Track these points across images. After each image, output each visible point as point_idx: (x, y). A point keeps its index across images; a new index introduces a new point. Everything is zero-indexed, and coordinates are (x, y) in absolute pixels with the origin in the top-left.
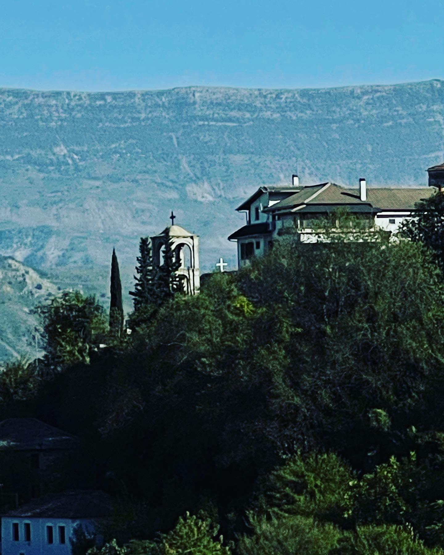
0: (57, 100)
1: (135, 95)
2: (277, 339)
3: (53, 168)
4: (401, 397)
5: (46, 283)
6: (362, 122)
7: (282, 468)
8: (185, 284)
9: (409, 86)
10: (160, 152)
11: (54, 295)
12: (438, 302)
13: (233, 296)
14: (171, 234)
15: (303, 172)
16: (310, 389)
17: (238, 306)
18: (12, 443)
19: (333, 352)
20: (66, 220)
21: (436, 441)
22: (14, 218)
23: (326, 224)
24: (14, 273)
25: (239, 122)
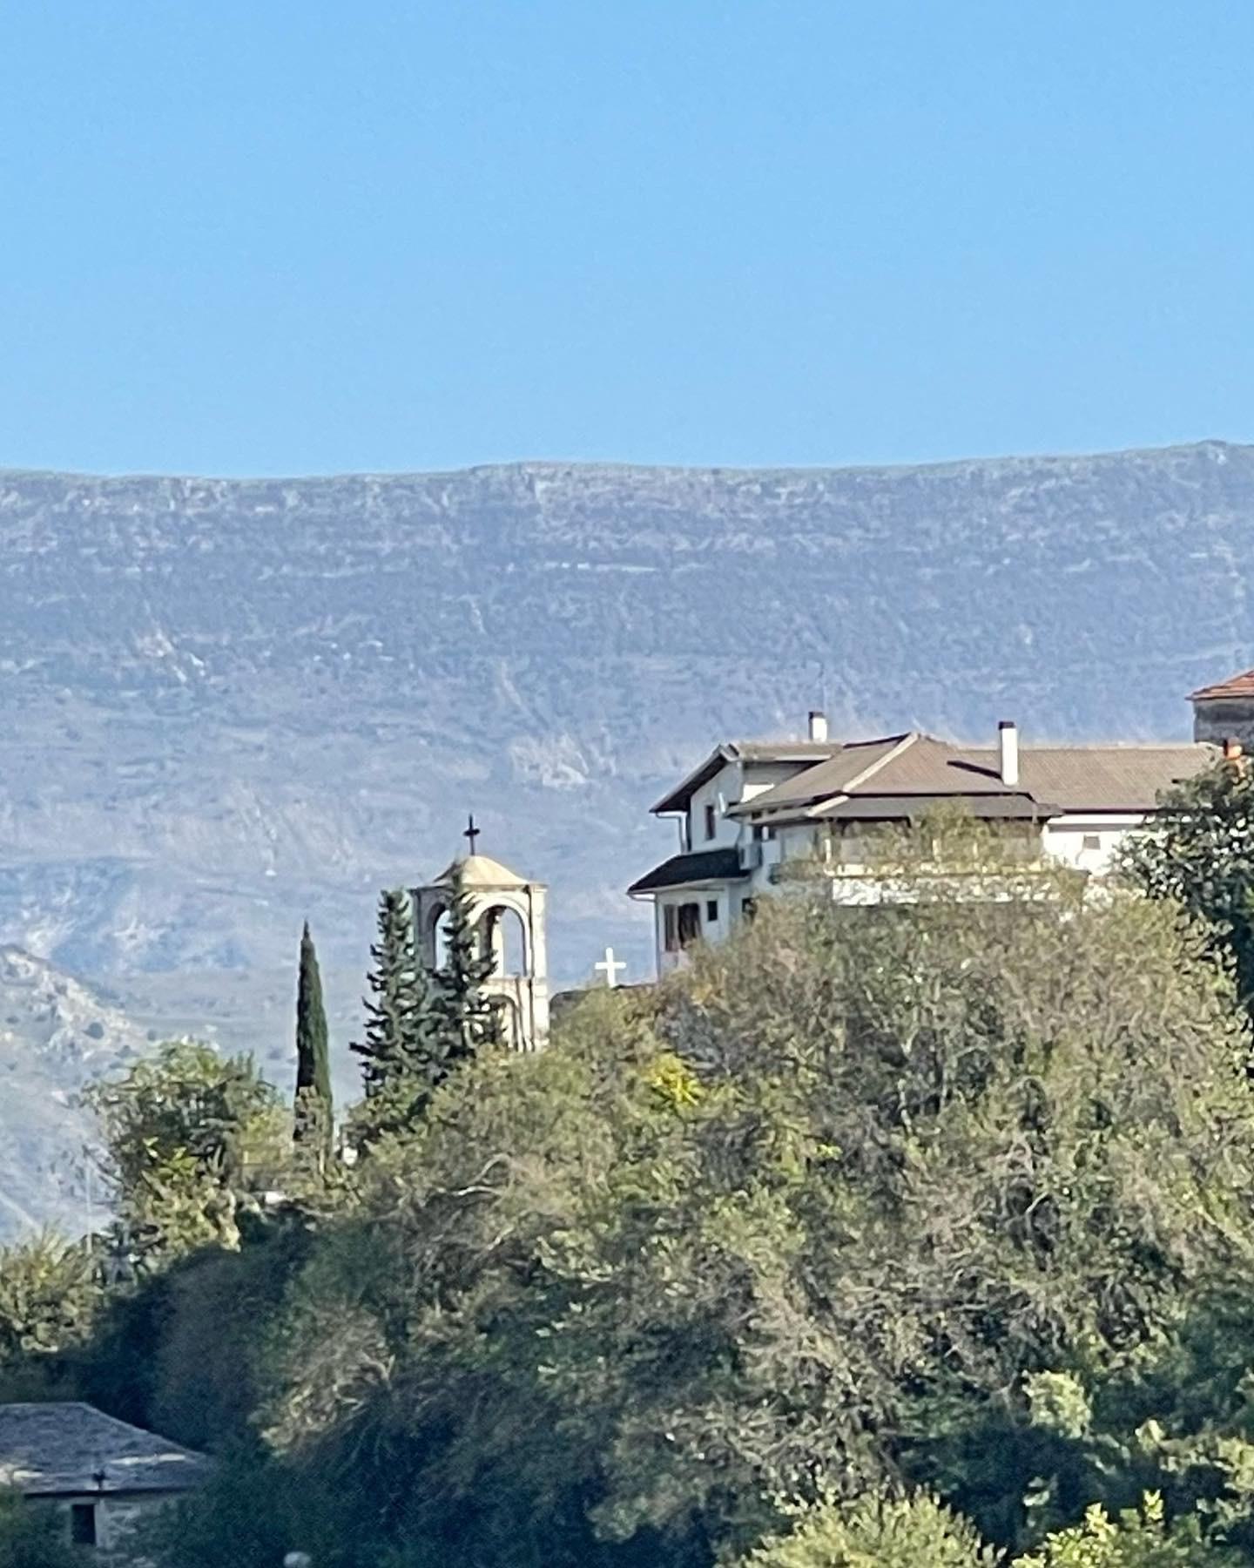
0: (143, 502)
1: (365, 487)
2: (768, 1177)
3: (132, 694)
4: (1118, 1340)
5: (114, 1021)
6: (1007, 561)
7: (783, 1541)
8: (507, 1022)
9: (1139, 461)
10: (434, 649)
11: (136, 1055)
12: (1221, 1070)
13: (643, 1055)
14: (467, 879)
15: (839, 704)
16: (862, 1317)
17: (659, 1082)
18: (18, 1475)
19: (924, 1214)
20: (170, 840)
21: (1219, 1464)
22: (26, 838)
23: (905, 852)
24: (24, 991)
25: (659, 564)
